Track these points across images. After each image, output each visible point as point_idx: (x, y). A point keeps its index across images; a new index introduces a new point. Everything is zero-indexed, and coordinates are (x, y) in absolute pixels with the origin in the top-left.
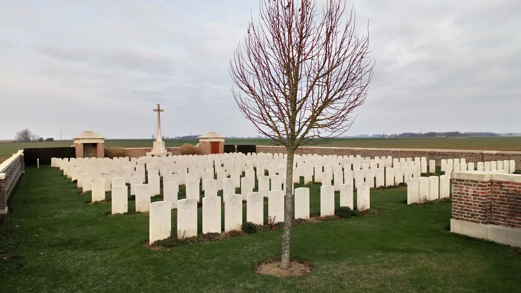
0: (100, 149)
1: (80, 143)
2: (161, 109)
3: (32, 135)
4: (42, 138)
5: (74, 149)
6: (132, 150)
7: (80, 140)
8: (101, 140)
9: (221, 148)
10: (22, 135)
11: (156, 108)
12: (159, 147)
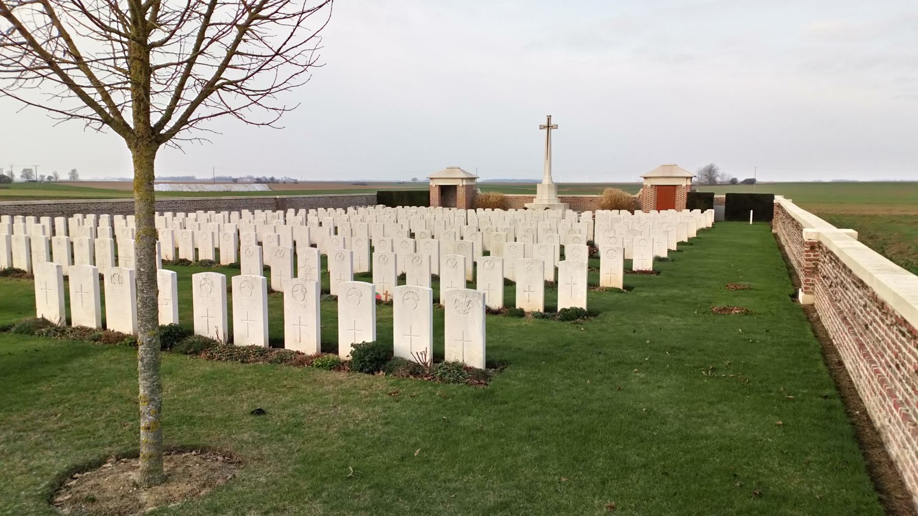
0: (461, 194)
1: (434, 185)
2: (553, 123)
3: (719, 174)
4: (736, 179)
5: (427, 194)
6: (517, 198)
7: (435, 180)
8: (461, 180)
9: (681, 198)
10: (705, 174)
11: (545, 124)
12: (544, 196)
